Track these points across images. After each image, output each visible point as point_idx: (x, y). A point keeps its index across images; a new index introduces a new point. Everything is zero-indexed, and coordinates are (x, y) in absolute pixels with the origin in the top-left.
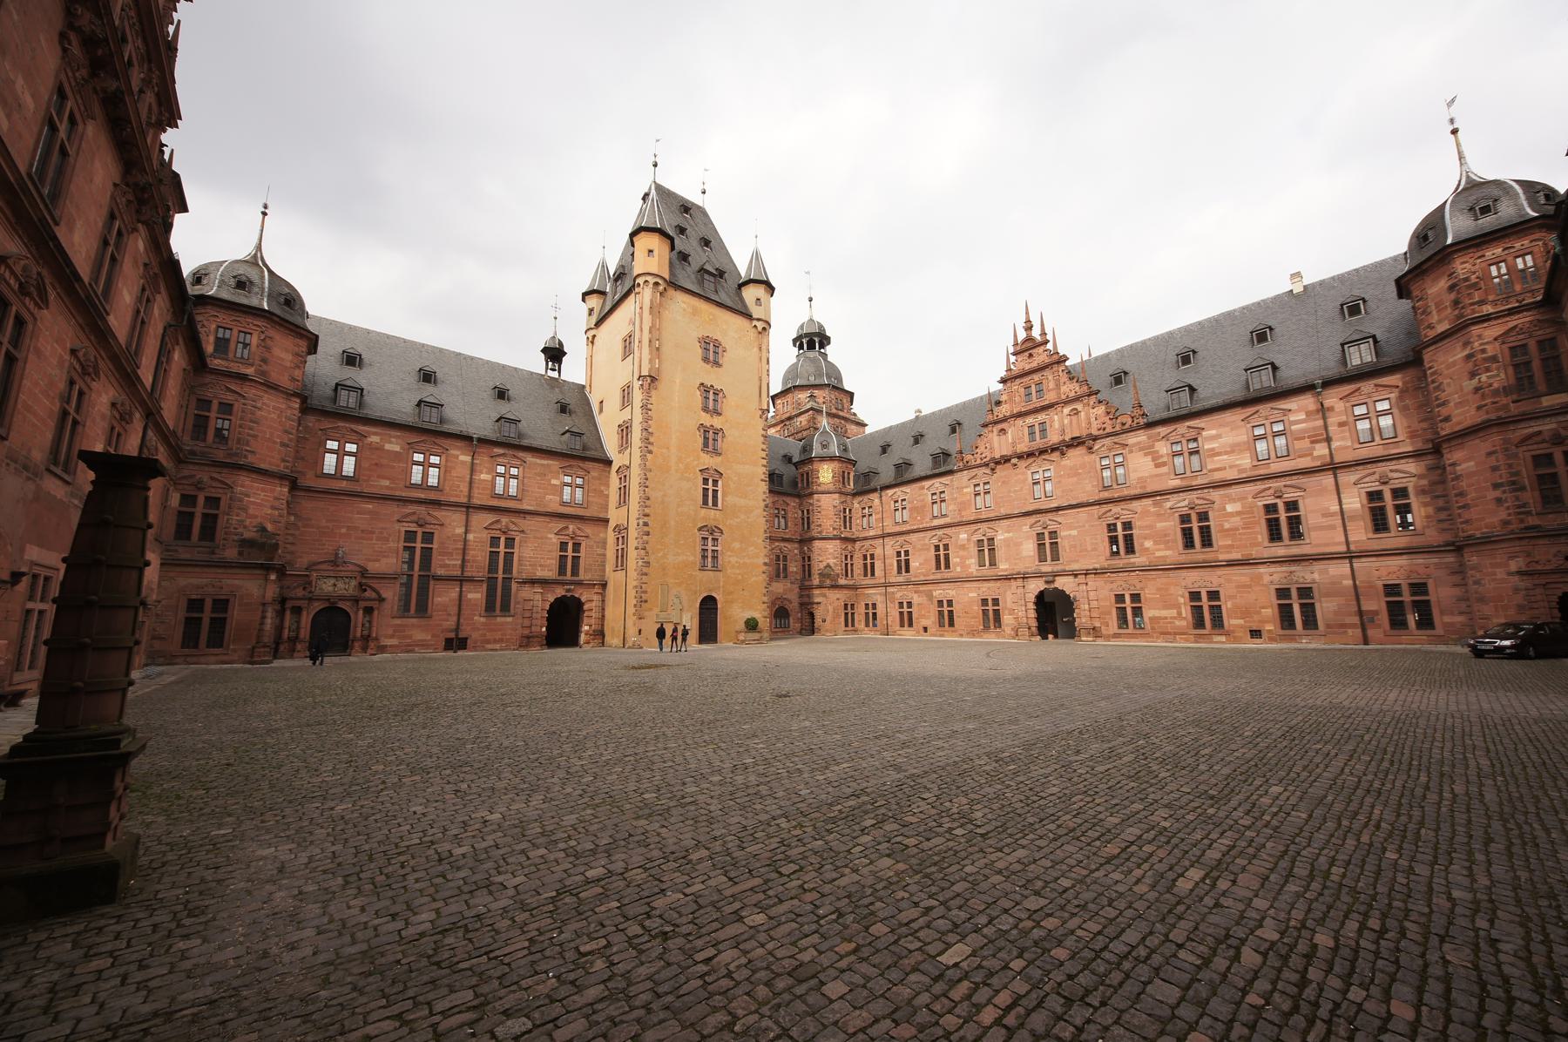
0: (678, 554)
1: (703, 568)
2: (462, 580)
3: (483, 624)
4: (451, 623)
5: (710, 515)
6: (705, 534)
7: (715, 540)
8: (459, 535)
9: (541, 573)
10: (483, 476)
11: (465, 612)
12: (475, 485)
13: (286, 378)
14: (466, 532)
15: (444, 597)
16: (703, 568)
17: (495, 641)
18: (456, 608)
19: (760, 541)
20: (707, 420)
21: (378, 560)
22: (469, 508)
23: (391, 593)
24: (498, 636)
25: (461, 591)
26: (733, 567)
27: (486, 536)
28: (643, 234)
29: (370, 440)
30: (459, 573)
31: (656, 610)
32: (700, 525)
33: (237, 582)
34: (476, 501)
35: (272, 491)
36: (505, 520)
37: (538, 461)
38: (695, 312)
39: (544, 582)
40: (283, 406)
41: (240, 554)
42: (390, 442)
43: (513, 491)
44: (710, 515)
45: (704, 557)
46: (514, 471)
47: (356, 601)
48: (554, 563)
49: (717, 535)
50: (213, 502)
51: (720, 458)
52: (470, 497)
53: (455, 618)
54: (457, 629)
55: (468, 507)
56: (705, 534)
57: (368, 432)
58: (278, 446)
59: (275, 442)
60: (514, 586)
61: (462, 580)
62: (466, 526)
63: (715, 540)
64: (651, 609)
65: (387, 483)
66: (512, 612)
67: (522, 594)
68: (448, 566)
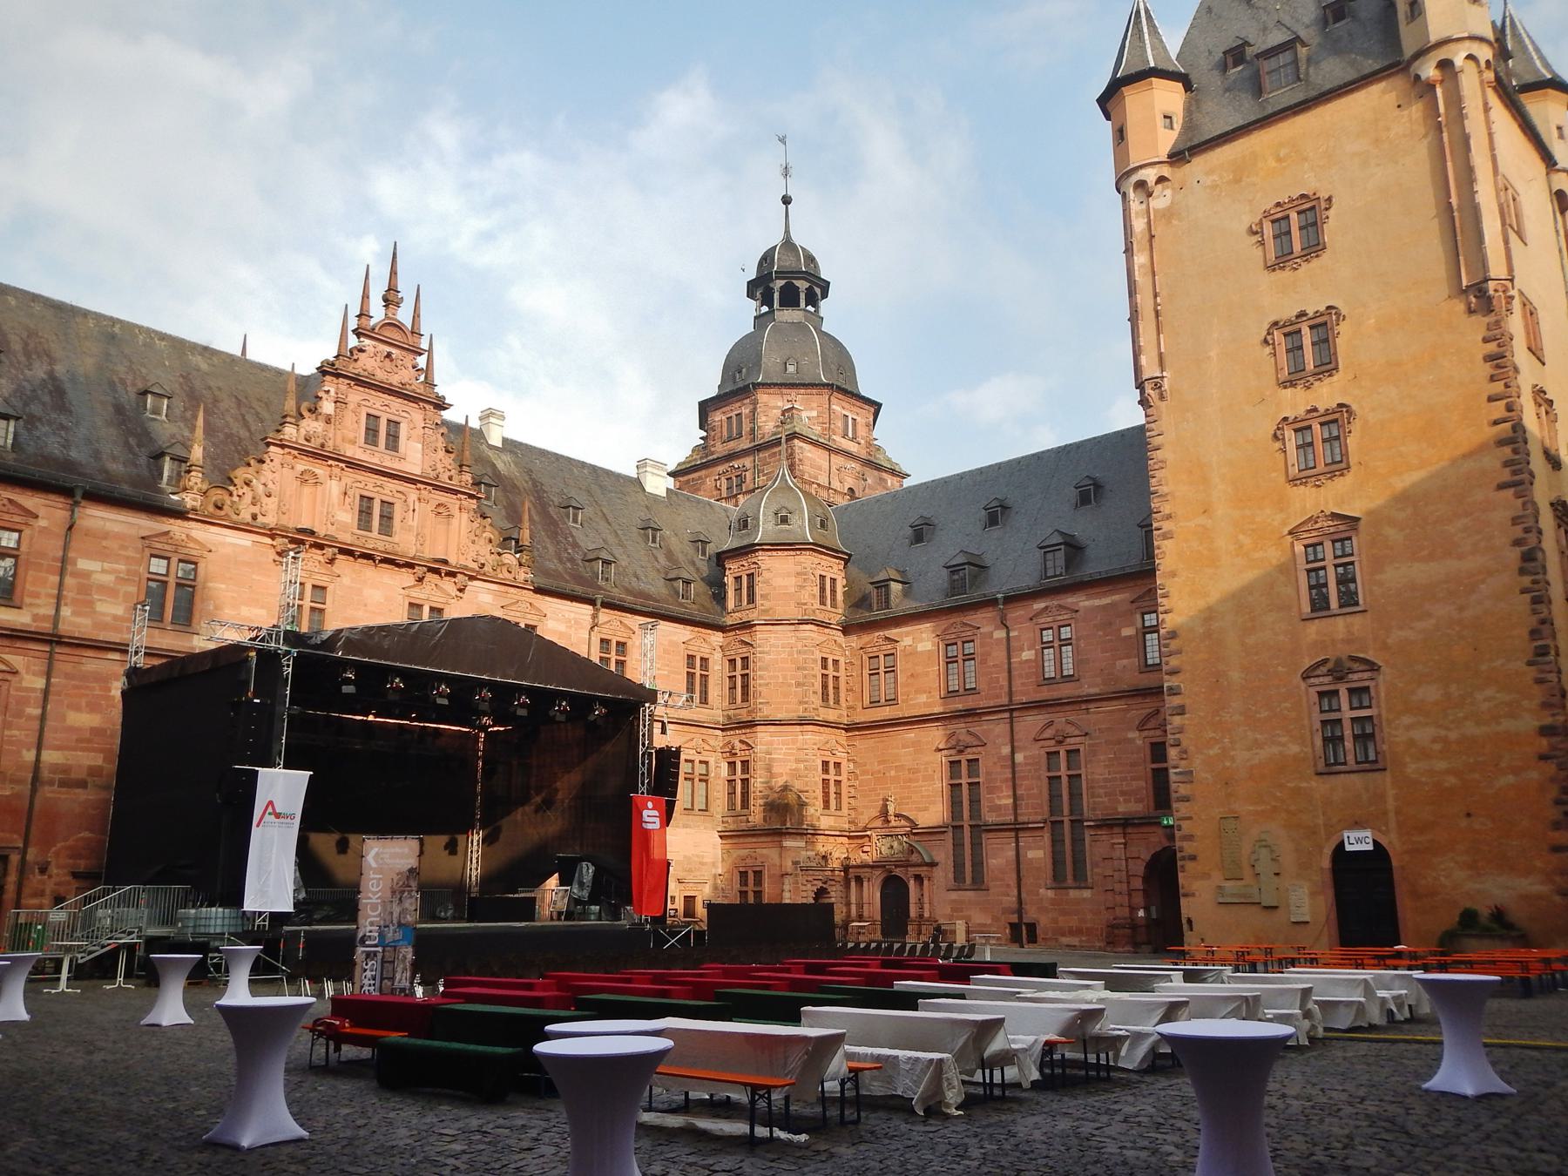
0: (1257, 744)
1: (1330, 767)
2: (1017, 828)
3: (1053, 902)
4: (1011, 900)
5: (1339, 630)
6: (1325, 682)
7: (1359, 693)
8: (1001, 758)
9: (1124, 808)
10: (1028, 655)
11: (1028, 881)
12: (1014, 673)
13: (792, 604)
14: (1013, 753)
15: (998, 856)
16: (1330, 767)
17: (1071, 932)
18: (1014, 876)
19: (1519, 665)
20: (1295, 402)
21: (926, 809)
22: (1012, 710)
23: (942, 853)
24: (1074, 922)
25: (1017, 846)
26: (1425, 754)
27: (1038, 752)
28: (1109, 106)
29: (902, 644)
30: (1012, 818)
31: (1217, 878)
32: (1307, 663)
33: (765, 851)
34: (1017, 698)
35: (794, 742)
36: (1060, 719)
37: (1097, 602)
38: (1239, 174)
39: (1126, 823)
40: (793, 641)
41: (765, 820)
42: (922, 640)
43: (1068, 669)
44: (1339, 630)
45: (1333, 741)
46: (1066, 633)
47: (906, 864)
48: (1143, 785)
49: (1358, 678)
50: (745, 763)
51: (1349, 478)
52: (1010, 693)
53: (1015, 892)
54: (1020, 911)
55: (1012, 710)
56: (1325, 682)
57: (901, 635)
58: (794, 689)
59: (790, 685)
60: (1087, 834)
61: (1017, 828)
62: (1012, 741)
63: (1359, 693)
64: (1206, 876)
65: (923, 698)
66: (1090, 880)
67: (1099, 847)
68: (999, 807)
